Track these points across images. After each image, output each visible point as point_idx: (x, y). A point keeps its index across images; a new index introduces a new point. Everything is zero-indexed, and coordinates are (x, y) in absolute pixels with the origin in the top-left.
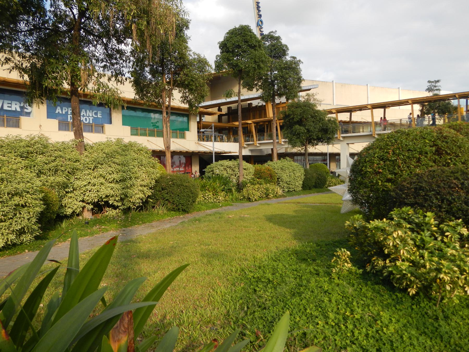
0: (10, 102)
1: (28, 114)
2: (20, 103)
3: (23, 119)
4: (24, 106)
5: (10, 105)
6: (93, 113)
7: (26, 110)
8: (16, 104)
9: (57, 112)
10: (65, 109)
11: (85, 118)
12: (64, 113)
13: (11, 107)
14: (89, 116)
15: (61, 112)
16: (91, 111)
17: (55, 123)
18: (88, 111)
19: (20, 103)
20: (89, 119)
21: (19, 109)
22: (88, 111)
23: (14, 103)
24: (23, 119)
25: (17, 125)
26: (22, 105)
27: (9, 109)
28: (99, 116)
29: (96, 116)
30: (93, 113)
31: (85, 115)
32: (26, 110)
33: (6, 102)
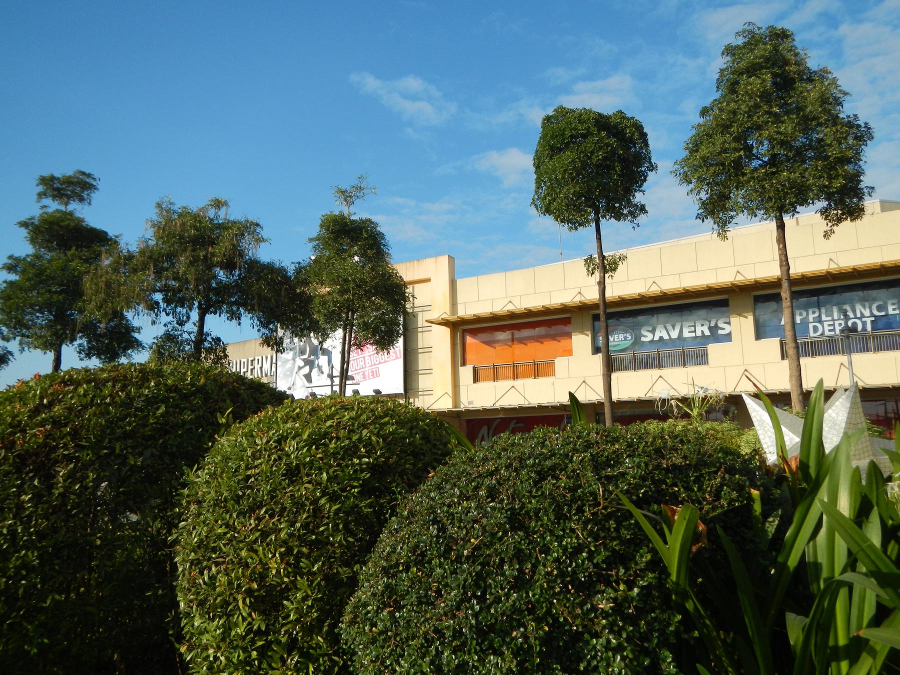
1: (728, 337)
3: (713, 349)
4: (716, 324)
5: (693, 329)
6: (874, 307)
7: (720, 332)
8: (702, 325)
10: (801, 314)
14: (863, 316)
17: (772, 345)
18: (859, 308)
19: (710, 322)
20: (864, 323)
21: (707, 333)
22: (859, 308)
24: (713, 349)
25: (702, 358)
26: (713, 324)
27: (693, 335)
28: (891, 312)
29: (883, 313)
30: (874, 307)
32: (720, 332)
33: (686, 324)
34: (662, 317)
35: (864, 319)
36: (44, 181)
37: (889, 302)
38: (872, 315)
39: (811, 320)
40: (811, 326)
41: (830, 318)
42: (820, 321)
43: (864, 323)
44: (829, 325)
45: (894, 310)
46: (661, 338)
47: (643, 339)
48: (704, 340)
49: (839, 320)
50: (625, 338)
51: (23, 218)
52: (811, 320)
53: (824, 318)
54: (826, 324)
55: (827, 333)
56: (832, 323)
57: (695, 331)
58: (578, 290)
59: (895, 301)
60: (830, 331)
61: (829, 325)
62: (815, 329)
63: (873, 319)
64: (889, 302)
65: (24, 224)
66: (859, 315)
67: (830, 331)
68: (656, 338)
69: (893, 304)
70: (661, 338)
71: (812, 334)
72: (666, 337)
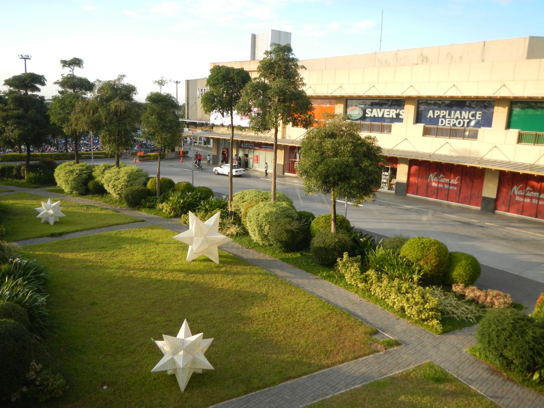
0: (388, 110)
2: (396, 110)
3: (395, 126)
7: (400, 117)
9: (428, 116)
11: (458, 120)
12: (435, 117)
13: (389, 115)
14: (464, 118)
15: (432, 117)
16: (467, 112)
19: (396, 110)
20: (464, 122)
21: (395, 116)
23: (392, 110)
26: (397, 112)
27: (388, 116)
31: (459, 117)
34: (375, 106)
35: (464, 120)
36: (62, 61)
37: (478, 113)
38: (468, 118)
39: (441, 117)
40: (440, 120)
41: (449, 117)
42: (445, 119)
43: (464, 122)
44: (449, 121)
45: (479, 117)
46: (374, 116)
47: (367, 115)
48: (392, 120)
49: (453, 118)
50: (359, 113)
51: (55, 81)
52: (441, 117)
53: (447, 117)
54: (447, 120)
55: (447, 125)
56: (450, 120)
57: (389, 115)
58: (340, 86)
59: (481, 112)
60: (448, 124)
61: (449, 121)
62: (442, 122)
63: (468, 120)
64: (478, 113)
65: (56, 83)
66: (462, 118)
67: (448, 124)
68: (372, 116)
69: (480, 114)
70: (374, 116)
71: (440, 124)
72: (376, 116)
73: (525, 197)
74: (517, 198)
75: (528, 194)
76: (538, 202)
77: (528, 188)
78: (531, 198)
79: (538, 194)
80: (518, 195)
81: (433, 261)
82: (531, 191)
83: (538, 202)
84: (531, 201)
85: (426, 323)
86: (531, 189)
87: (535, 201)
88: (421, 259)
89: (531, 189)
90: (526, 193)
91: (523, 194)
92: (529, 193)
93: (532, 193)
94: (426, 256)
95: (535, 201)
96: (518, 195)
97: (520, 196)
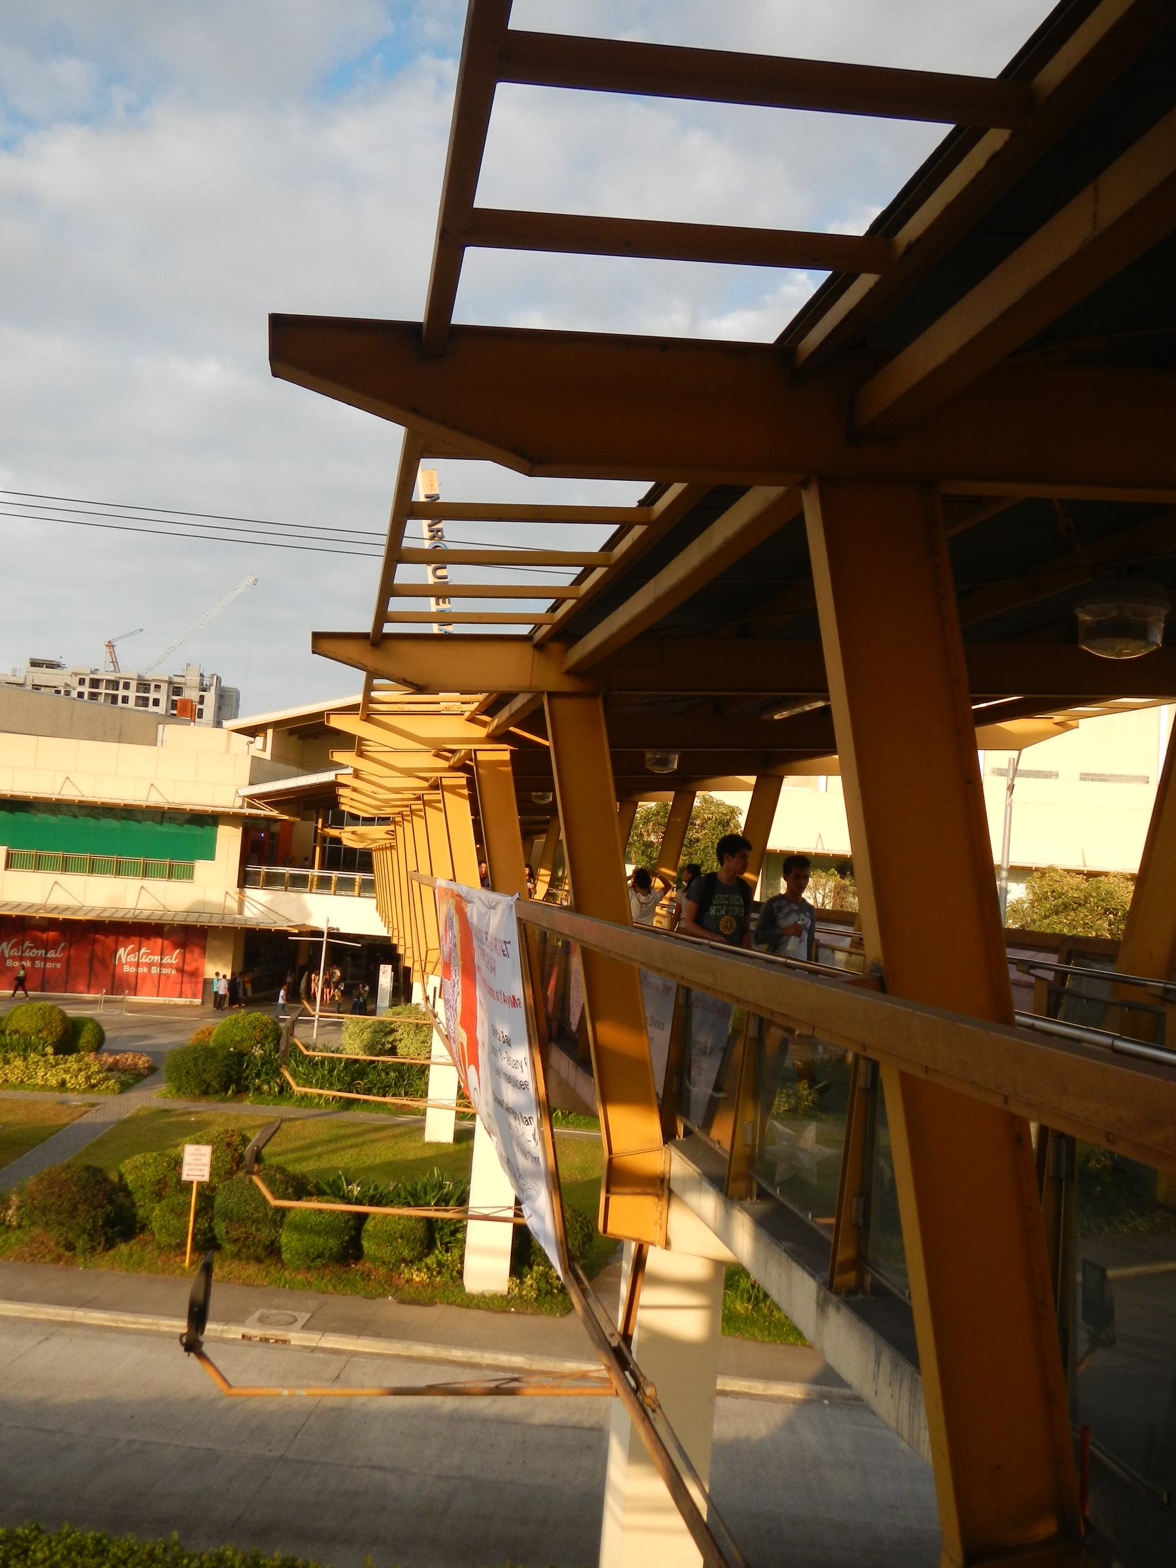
73: (21, 958)
74: (9, 963)
75: (27, 954)
76: (45, 965)
77: (27, 944)
78: (33, 960)
79: (43, 951)
80: (10, 957)
81: (59, 1028)
82: (31, 948)
83: (45, 965)
84: (33, 964)
85: (96, 1088)
86: (32, 945)
87: (39, 964)
88: (43, 1029)
89: (32, 945)
90: (23, 952)
91: (20, 953)
92: (30, 952)
93: (34, 950)
94: (49, 1023)
95: (39, 964)
96: (10, 957)
97: (14, 958)
